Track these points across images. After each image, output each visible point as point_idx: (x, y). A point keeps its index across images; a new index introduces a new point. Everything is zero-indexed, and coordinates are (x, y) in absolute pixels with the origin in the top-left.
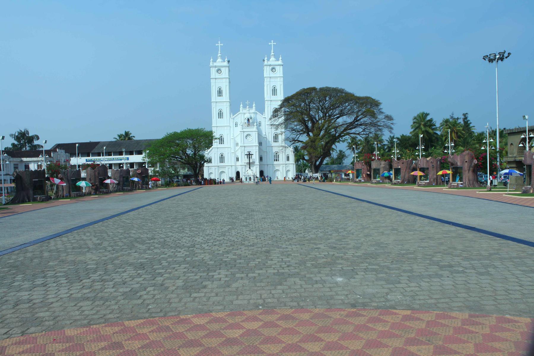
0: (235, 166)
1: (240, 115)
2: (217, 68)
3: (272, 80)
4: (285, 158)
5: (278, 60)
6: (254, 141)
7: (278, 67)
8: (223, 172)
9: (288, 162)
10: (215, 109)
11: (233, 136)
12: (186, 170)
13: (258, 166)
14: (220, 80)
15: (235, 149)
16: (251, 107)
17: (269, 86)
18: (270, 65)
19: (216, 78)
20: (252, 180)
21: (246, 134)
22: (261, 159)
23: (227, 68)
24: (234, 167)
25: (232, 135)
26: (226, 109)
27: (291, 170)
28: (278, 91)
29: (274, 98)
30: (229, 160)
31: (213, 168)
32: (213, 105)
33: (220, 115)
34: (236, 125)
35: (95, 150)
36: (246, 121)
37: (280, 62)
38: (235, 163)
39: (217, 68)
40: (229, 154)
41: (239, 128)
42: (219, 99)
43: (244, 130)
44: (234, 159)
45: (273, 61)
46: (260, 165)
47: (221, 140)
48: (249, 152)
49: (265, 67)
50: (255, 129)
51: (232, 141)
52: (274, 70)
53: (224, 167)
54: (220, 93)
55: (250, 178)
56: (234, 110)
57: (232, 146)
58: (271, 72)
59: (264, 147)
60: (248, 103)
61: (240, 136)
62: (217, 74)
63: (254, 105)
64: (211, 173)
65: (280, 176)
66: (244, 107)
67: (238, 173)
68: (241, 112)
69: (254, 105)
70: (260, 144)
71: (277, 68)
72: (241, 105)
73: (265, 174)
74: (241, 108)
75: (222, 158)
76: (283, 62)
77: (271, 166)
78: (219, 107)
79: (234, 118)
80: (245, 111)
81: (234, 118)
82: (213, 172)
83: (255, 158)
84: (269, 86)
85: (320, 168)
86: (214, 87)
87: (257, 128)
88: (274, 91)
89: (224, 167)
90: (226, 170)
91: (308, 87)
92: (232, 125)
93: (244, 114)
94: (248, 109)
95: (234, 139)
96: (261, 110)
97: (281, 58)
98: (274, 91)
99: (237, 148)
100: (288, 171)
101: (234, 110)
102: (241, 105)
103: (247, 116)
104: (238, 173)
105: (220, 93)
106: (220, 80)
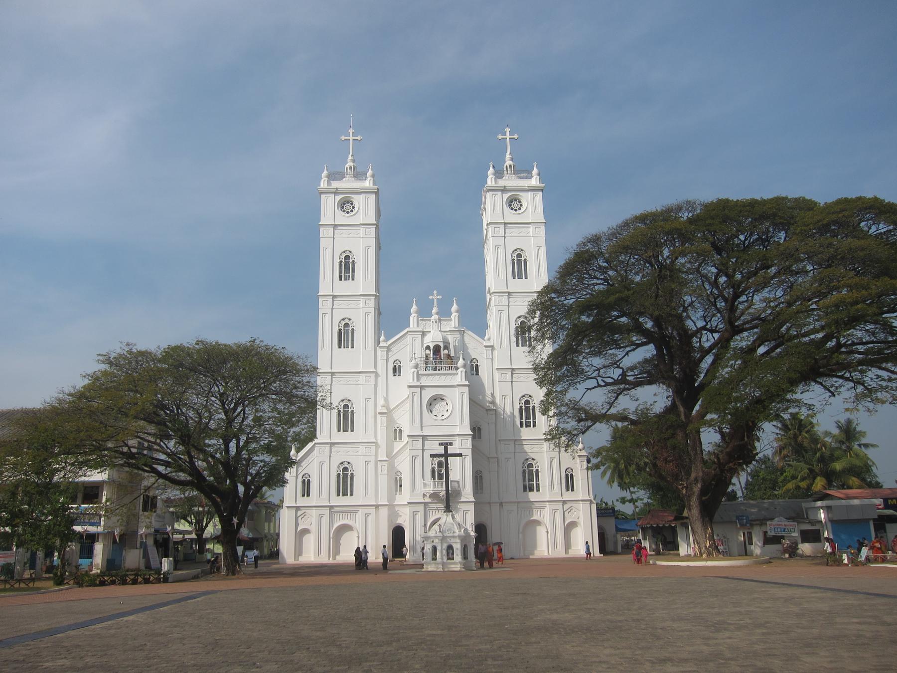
0: (391, 506)
1: (409, 338)
2: (339, 197)
4: (558, 480)
6: (455, 420)
7: (530, 194)
8: (345, 528)
9: (568, 496)
10: (328, 318)
11: (386, 406)
13: (471, 507)
14: (349, 232)
16: (444, 313)
17: (501, 250)
18: (504, 190)
19: (335, 226)
20: (458, 557)
21: (428, 394)
24: (384, 512)
25: (381, 402)
27: (581, 521)
28: (532, 267)
29: (517, 285)
31: (314, 513)
32: (324, 306)
33: (345, 337)
34: (397, 370)
36: (431, 353)
37: (534, 181)
38: (391, 498)
39: (339, 197)
41: (408, 374)
42: (344, 287)
43: (424, 381)
46: (477, 504)
47: (346, 420)
49: (488, 194)
50: (459, 377)
51: (382, 421)
53: (352, 510)
54: (347, 268)
56: (389, 321)
58: (507, 209)
60: (435, 296)
61: (408, 405)
62: (339, 213)
63: (455, 307)
65: (546, 545)
66: (424, 313)
67: (398, 533)
68: (413, 326)
69: (455, 307)
70: (477, 431)
71: (527, 198)
72: (414, 308)
73: (494, 536)
75: (345, 482)
76: (541, 180)
79: (388, 349)
82: (314, 528)
83: (461, 471)
86: (329, 252)
88: (519, 266)
89: (352, 510)
90: (357, 521)
95: (389, 413)
96: (475, 320)
98: (519, 266)
99: (398, 445)
100: (569, 528)
101: (389, 321)
102: (414, 308)
103: (433, 337)
104: (398, 533)
105: (347, 268)
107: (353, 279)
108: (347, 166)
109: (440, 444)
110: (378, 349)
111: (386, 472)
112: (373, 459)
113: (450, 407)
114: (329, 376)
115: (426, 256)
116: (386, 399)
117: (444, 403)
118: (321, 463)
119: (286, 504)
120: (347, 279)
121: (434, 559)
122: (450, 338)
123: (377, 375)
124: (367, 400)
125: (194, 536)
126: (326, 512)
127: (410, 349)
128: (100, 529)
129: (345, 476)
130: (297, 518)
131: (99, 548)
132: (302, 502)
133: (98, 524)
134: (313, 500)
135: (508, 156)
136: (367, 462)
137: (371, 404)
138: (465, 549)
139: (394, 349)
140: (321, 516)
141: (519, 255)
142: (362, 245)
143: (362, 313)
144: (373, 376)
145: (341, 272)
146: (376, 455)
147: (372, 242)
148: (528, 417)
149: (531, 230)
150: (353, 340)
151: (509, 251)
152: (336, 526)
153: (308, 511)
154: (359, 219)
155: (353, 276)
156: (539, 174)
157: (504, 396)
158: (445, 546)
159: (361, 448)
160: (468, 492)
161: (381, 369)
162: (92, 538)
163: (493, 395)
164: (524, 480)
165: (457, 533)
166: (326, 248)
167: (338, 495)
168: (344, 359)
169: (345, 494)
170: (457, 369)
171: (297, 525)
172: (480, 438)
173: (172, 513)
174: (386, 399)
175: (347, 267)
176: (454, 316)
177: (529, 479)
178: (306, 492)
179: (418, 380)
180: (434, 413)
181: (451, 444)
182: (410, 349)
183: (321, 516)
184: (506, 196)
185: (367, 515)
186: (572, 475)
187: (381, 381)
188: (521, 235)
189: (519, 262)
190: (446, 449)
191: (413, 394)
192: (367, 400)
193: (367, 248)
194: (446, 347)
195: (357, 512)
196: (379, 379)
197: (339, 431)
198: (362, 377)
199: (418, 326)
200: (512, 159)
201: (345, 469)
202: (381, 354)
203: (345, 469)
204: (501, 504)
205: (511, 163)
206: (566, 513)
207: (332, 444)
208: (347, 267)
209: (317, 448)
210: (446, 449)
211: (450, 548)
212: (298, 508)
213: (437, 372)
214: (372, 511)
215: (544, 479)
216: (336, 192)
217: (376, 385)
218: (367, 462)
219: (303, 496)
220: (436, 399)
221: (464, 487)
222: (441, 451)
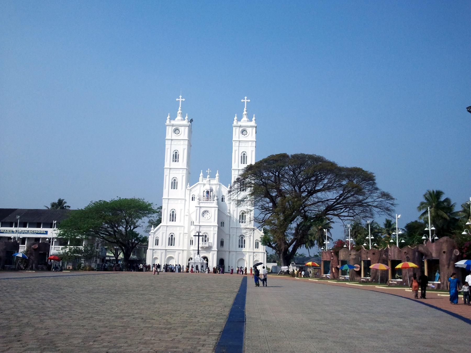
0: (188, 251)
1: (198, 186)
3: (242, 144)
5: (251, 121)
6: (212, 220)
7: (251, 129)
8: (171, 258)
9: (256, 250)
11: (189, 212)
13: (216, 252)
14: (177, 141)
15: (189, 228)
16: (213, 177)
17: (237, 152)
18: (240, 126)
19: (172, 140)
22: (221, 243)
24: (185, 253)
25: (186, 211)
26: (181, 177)
30: (182, 243)
31: (159, 251)
32: (166, 172)
33: (174, 185)
34: (193, 199)
35: (8, 219)
36: (205, 193)
37: (253, 123)
38: (189, 248)
39: (174, 128)
40: (182, 235)
42: (174, 165)
44: (187, 242)
45: (244, 121)
46: (218, 251)
47: (173, 217)
50: (214, 204)
51: (187, 218)
52: (244, 133)
53: (174, 251)
54: (176, 157)
55: (197, 267)
56: (192, 180)
57: (186, 224)
58: (241, 135)
60: (208, 171)
61: (195, 213)
62: (174, 134)
63: (217, 175)
64: (156, 258)
66: (205, 177)
69: (217, 175)
70: (221, 224)
72: (201, 174)
74: (201, 178)
75: (171, 241)
76: (256, 123)
77: (235, 253)
78: (174, 174)
79: (190, 190)
80: (205, 181)
82: (159, 257)
83: (213, 240)
84: (237, 152)
86: (169, 150)
87: (218, 204)
90: (175, 256)
91: (311, 153)
92: (188, 198)
93: (204, 185)
94: (208, 179)
95: (189, 216)
97: (254, 118)
101: (192, 180)
102: (201, 174)
103: (207, 187)
105: (176, 157)
106: (177, 141)
108: (178, 112)
110: (187, 190)
112: (182, 232)
113: (210, 215)
114: (167, 200)
115: (206, 157)
116: (189, 210)
117: (208, 213)
118: (163, 233)
120: (176, 161)
122: (214, 188)
123: (185, 200)
124: (181, 210)
125: (114, 258)
126: (164, 251)
127: (199, 190)
129: (172, 238)
130: (153, 253)
132: (156, 247)
134: (159, 247)
135: (245, 109)
136: (180, 234)
139: (193, 190)
140: (162, 253)
141: (244, 154)
142: (182, 148)
143: (181, 175)
144: (184, 201)
147: (186, 147)
151: (241, 152)
152: (167, 257)
153: (157, 251)
154: (181, 137)
156: (255, 120)
157: (234, 211)
159: (178, 228)
160: (215, 248)
161: (187, 198)
163: (229, 210)
164: (239, 243)
166: (168, 149)
168: (174, 194)
169: (171, 245)
170: (214, 200)
171: (153, 256)
174: (189, 210)
176: (217, 178)
178: (157, 243)
179: (199, 204)
182: (199, 190)
183: (162, 253)
184: (241, 129)
185: (179, 253)
187: (187, 202)
189: (244, 157)
191: (197, 210)
192: (181, 210)
193: (184, 149)
194: (212, 190)
196: (186, 202)
198: (180, 201)
199: (202, 181)
200: (246, 111)
202: (188, 192)
204: (229, 252)
207: (167, 226)
212: (153, 250)
214: (181, 252)
216: (173, 126)
217: (185, 204)
218: (180, 234)
220: (205, 212)
221: (214, 245)
222: (197, 234)
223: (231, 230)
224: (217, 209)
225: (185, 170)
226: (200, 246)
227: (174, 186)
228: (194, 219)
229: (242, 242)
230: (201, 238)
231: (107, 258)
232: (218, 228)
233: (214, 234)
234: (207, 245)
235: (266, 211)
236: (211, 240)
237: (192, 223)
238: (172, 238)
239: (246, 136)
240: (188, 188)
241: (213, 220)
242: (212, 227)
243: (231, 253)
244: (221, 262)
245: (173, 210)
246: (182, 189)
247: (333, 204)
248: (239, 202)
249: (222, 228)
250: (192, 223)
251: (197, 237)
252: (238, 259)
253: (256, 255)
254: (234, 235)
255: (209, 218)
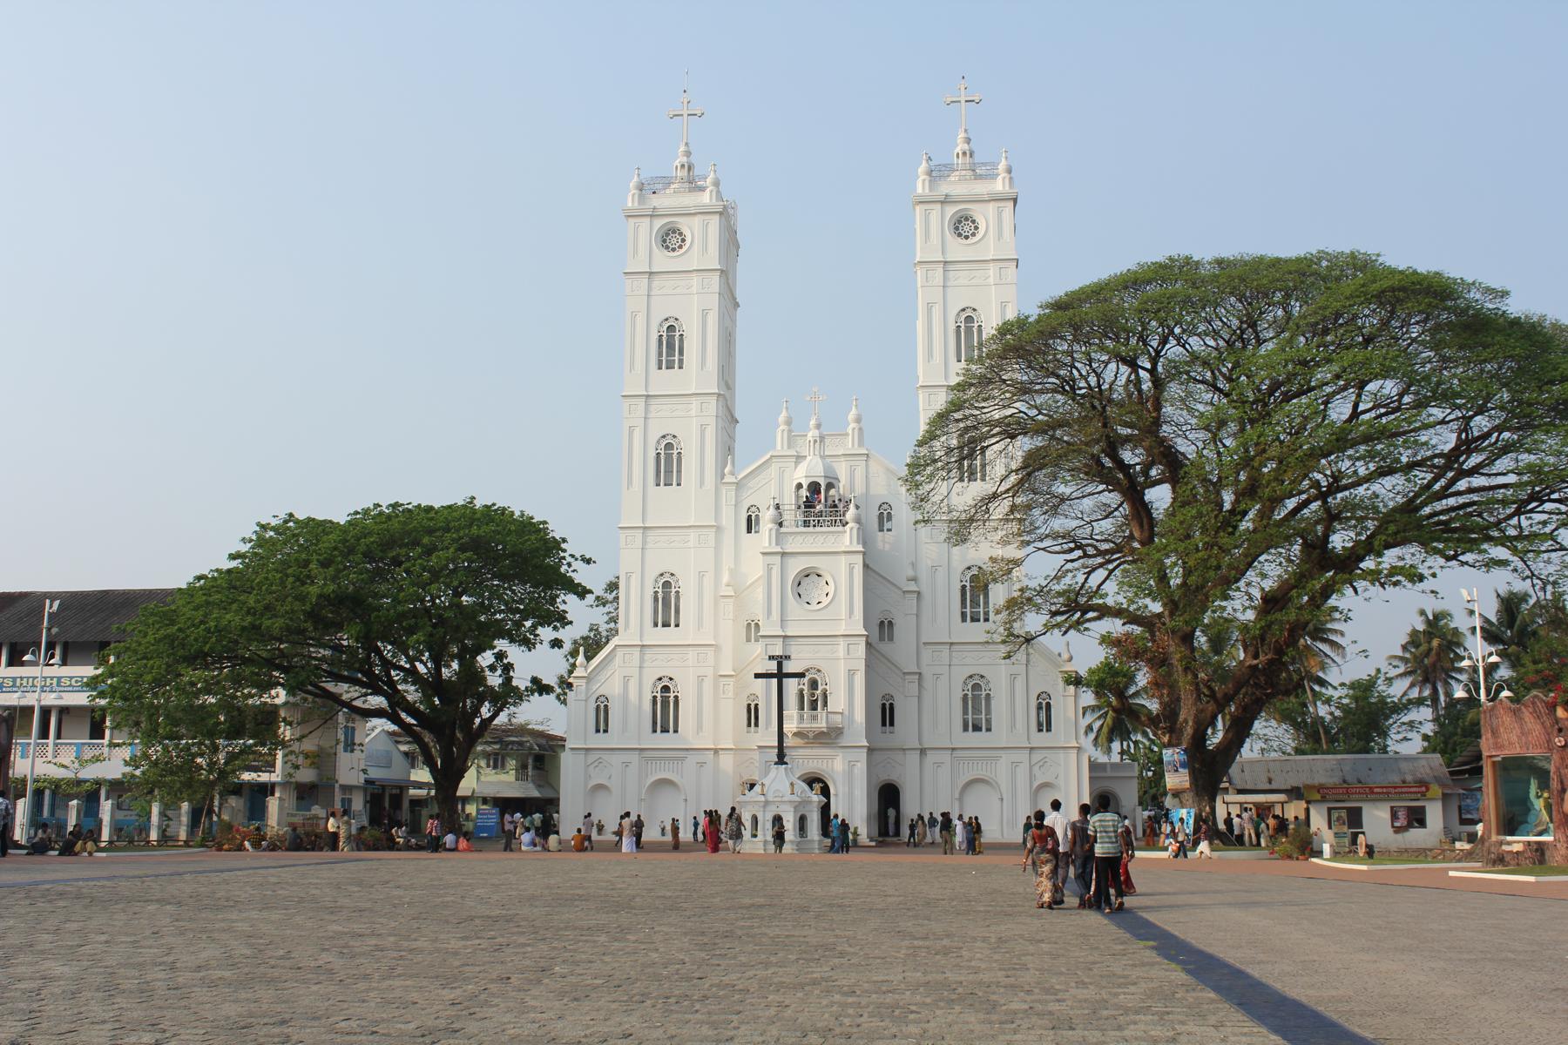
1: (773, 469)
2: (658, 223)
4: (1026, 715)
7: (992, 207)
12: (510, 777)
13: (863, 754)
17: (937, 312)
18: (946, 201)
21: (796, 566)
22: (887, 715)
23: (715, 221)
25: (725, 578)
40: (708, 685)
47: (666, 608)
48: (780, 660)
50: (847, 539)
57: (729, 632)
58: (950, 236)
59: (902, 649)
70: (882, 630)
71: (985, 216)
79: (739, 485)
81: (739, 485)
83: (848, 700)
84: (937, 312)
85: (1234, 770)
87: (865, 539)
92: (732, 521)
107: (681, 367)
109: (771, 658)
110: (724, 489)
111: (731, 694)
112: (710, 672)
119: (569, 745)
120: (670, 366)
121: (755, 836)
123: (718, 529)
124: (701, 575)
128: (275, 777)
131: (273, 804)
133: (270, 766)
136: (701, 679)
137: (708, 581)
138: (802, 822)
141: (969, 319)
144: (712, 533)
145: (660, 354)
146: (716, 668)
147: (713, 302)
148: (975, 603)
149: (991, 272)
150: (679, 471)
153: (606, 756)
155: (681, 361)
158: (770, 817)
159: (692, 653)
162: (266, 790)
164: (965, 712)
165: (788, 797)
167: (655, 731)
169: (665, 730)
171: (588, 777)
172: (891, 639)
173: (406, 754)
174: (733, 572)
175: (670, 346)
177: (976, 710)
180: (805, 598)
181: (788, 658)
184: (951, 210)
185: (702, 764)
186: (1048, 705)
188: (974, 282)
190: (780, 665)
191: (769, 568)
192: (701, 575)
193: (704, 314)
195: (683, 759)
197: (656, 625)
201: (666, 689)
202: (728, 494)
203: (666, 689)
204: (923, 751)
205: (966, 147)
206: (1036, 768)
208: (670, 346)
209: (620, 653)
210: (780, 665)
211: (778, 820)
213: (811, 529)
215: (1000, 710)
218: (701, 679)
219: (598, 731)
222: (772, 667)
223: (926, 654)
224: (859, 559)
225: (713, 400)
226: (790, 726)
227: (669, 472)
228: (760, 616)
229: (977, 710)
230: (791, 686)
231: (412, 792)
232: (868, 644)
233: (851, 673)
234: (822, 724)
235: (1086, 555)
236: (837, 702)
237: (752, 629)
238: (665, 702)
239: (972, 240)
240: (728, 479)
241: (844, 613)
242: (842, 642)
243: (931, 757)
244: (888, 796)
245: (667, 578)
246: (702, 483)
247: (1453, 482)
248: (961, 530)
249: (885, 647)
250: (752, 629)
251: (775, 681)
252: (960, 785)
253: (1044, 762)
254: (937, 676)
255: (826, 601)
